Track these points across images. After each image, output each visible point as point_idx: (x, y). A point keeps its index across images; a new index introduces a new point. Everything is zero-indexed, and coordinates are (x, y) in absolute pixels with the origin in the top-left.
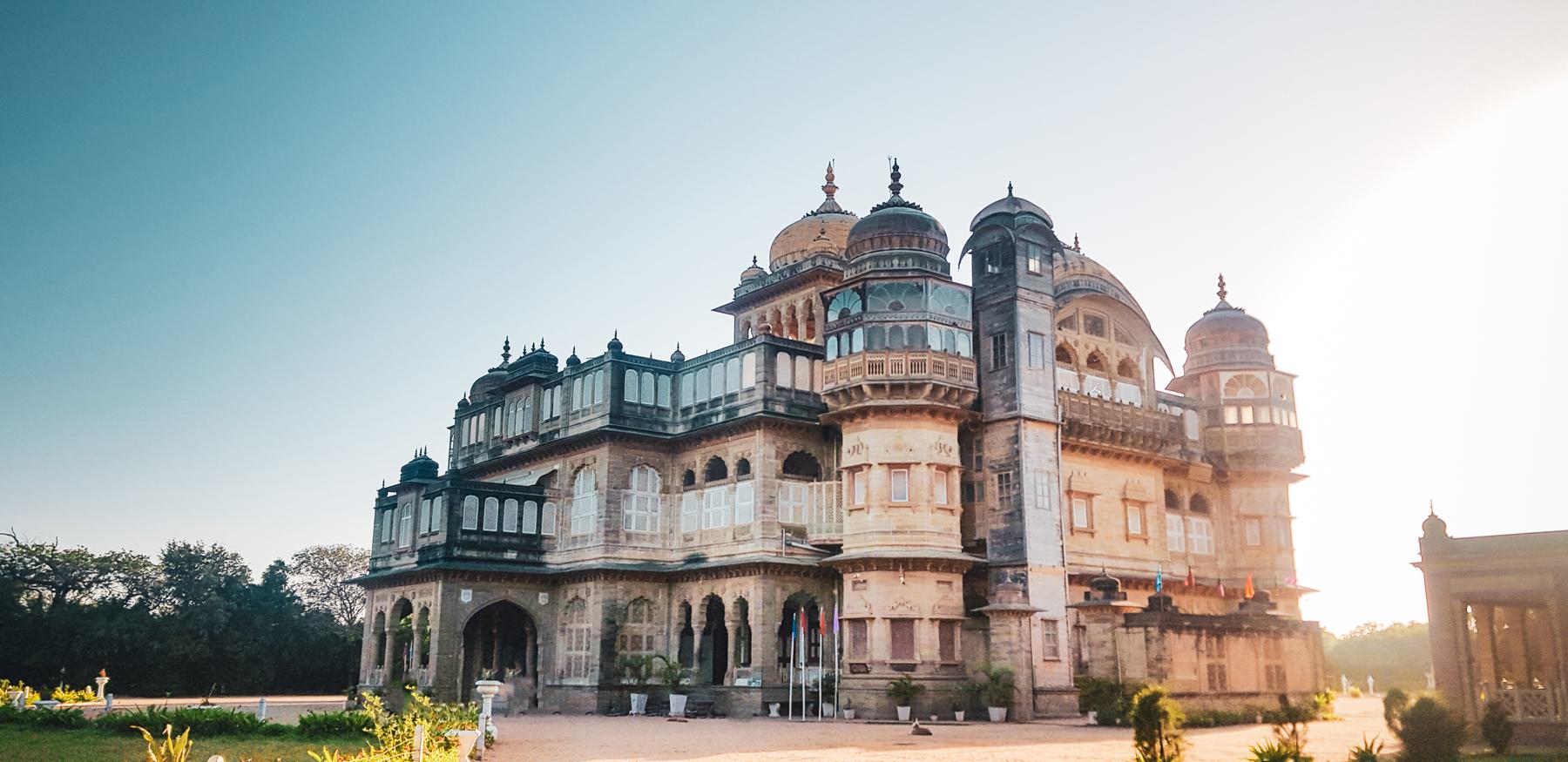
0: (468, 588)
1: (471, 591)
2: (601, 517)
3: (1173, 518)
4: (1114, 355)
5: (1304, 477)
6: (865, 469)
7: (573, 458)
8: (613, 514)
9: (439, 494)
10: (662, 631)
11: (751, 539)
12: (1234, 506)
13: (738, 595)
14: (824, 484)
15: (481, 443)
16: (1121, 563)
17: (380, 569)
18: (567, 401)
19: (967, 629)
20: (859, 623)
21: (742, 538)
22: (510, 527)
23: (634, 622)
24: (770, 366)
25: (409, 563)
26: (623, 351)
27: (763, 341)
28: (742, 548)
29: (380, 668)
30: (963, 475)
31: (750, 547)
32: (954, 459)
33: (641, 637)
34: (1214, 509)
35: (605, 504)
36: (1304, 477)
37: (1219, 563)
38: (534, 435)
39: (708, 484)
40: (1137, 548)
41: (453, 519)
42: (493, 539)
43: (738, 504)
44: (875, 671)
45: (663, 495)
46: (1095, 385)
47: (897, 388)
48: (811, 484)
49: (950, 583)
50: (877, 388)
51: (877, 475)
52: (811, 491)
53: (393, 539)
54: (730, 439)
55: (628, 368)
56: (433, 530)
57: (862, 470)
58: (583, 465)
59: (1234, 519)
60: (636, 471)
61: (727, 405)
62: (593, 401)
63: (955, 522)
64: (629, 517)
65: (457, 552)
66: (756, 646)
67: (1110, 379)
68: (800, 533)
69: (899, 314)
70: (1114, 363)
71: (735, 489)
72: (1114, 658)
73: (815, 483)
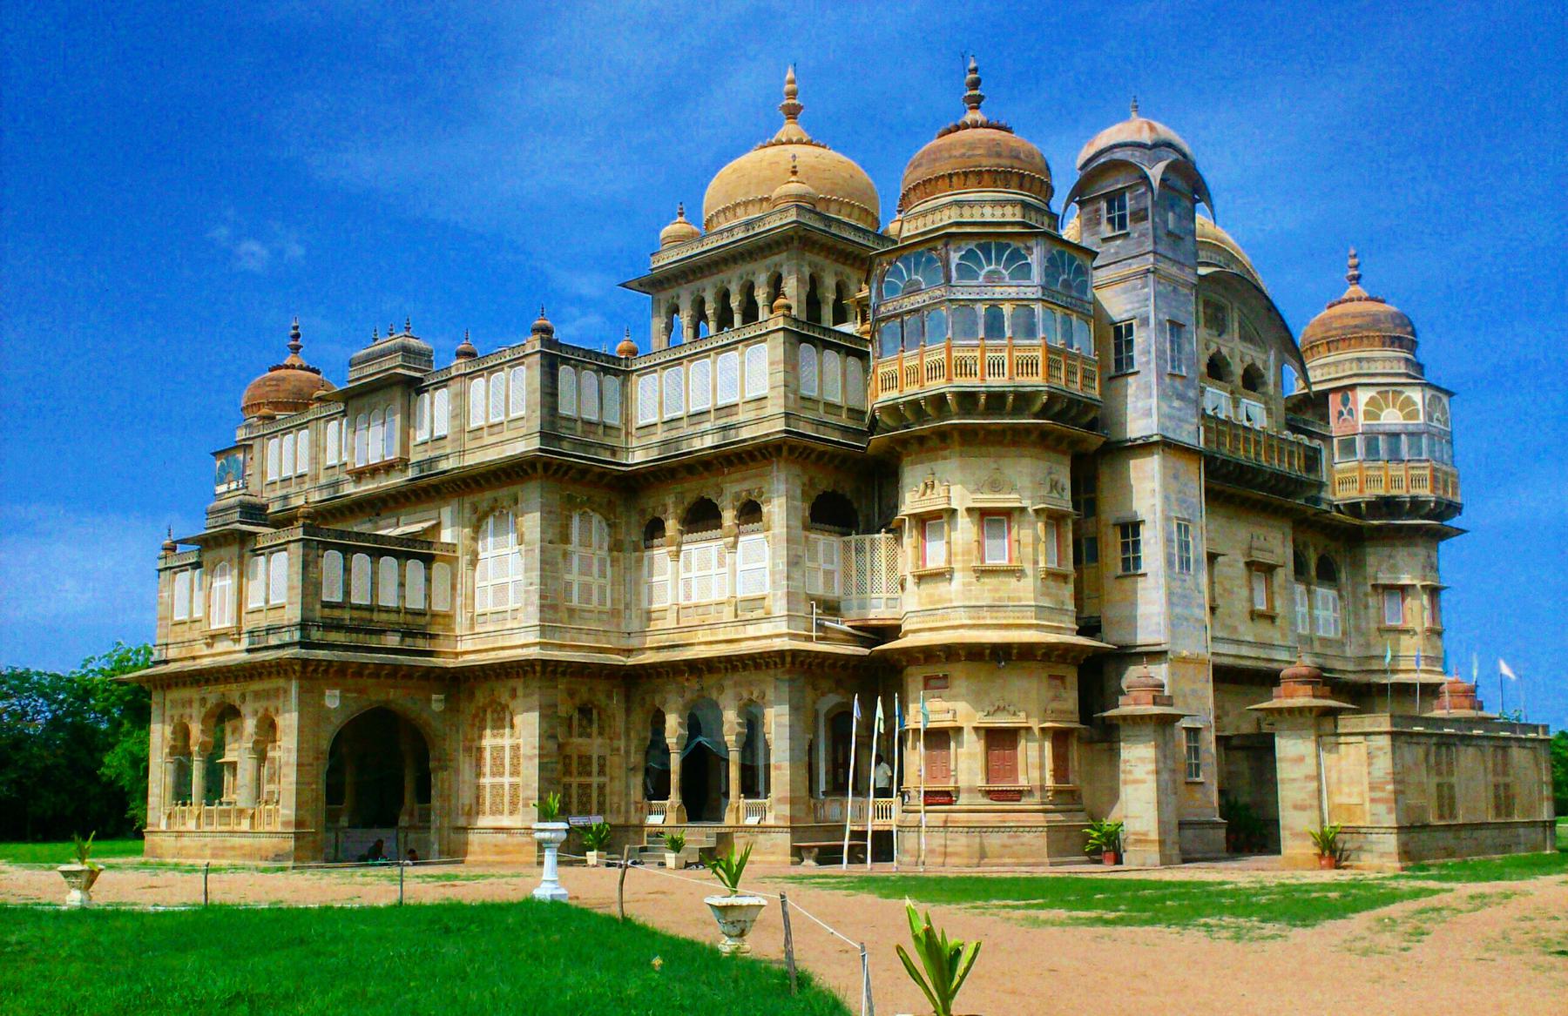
0: (335, 686)
1: (337, 692)
2: (531, 584)
3: (1300, 588)
4: (1237, 359)
5: (1460, 531)
6: (945, 518)
7: (477, 498)
8: (549, 582)
9: (282, 547)
10: (618, 749)
11: (768, 617)
12: (1370, 570)
13: (745, 695)
14: (868, 537)
15: (302, 476)
16: (1245, 651)
17: (175, 660)
18: (460, 412)
19: (1089, 742)
20: (939, 738)
21: (749, 616)
22: (388, 598)
23: (580, 736)
24: (791, 365)
25: (233, 653)
26: (554, 337)
27: (781, 326)
28: (751, 631)
29: (184, 804)
30: (1075, 523)
31: (765, 628)
32: (1065, 503)
33: (590, 758)
34: (1343, 576)
35: (538, 565)
36: (1460, 531)
37: (1347, 648)
38: (404, 463)
39: (686, 537)
40: (1265, 631)
41: (310, 585)
42: (366, 615)
43: (740, 567)
44: (963, 801)
45: (615, 553)
46: (1217, 399)
47: (996, 401)
48: (846, 538)
49: (1062, 678)
50: (967, 399)
51: (965, 530)
52: (847, 545)
53: (196, 615)
54: (726, 470)
55: (562, 364)
56: (272, 602)
57: (941, 517)
58: (493, 509)
59: (1369, 589)
60: (576, 522)
61: (722, 422)
62: (507, 415)
63: (1068, 590)
64: (569, 584)
65: (316, 635)
66: (778, 768)
67: (1232, 393)
68: (831, 608)
69: (997, 289)
70: (1238, 370)
71: (735, 545)
72: (1318, 777)
73: (854, 537)
